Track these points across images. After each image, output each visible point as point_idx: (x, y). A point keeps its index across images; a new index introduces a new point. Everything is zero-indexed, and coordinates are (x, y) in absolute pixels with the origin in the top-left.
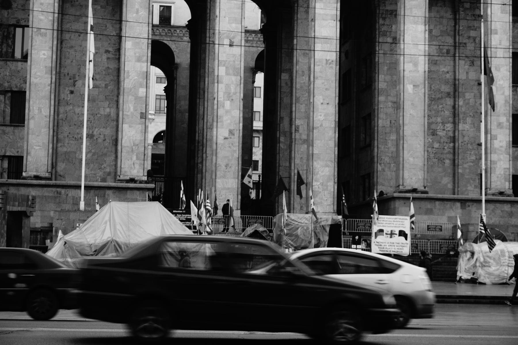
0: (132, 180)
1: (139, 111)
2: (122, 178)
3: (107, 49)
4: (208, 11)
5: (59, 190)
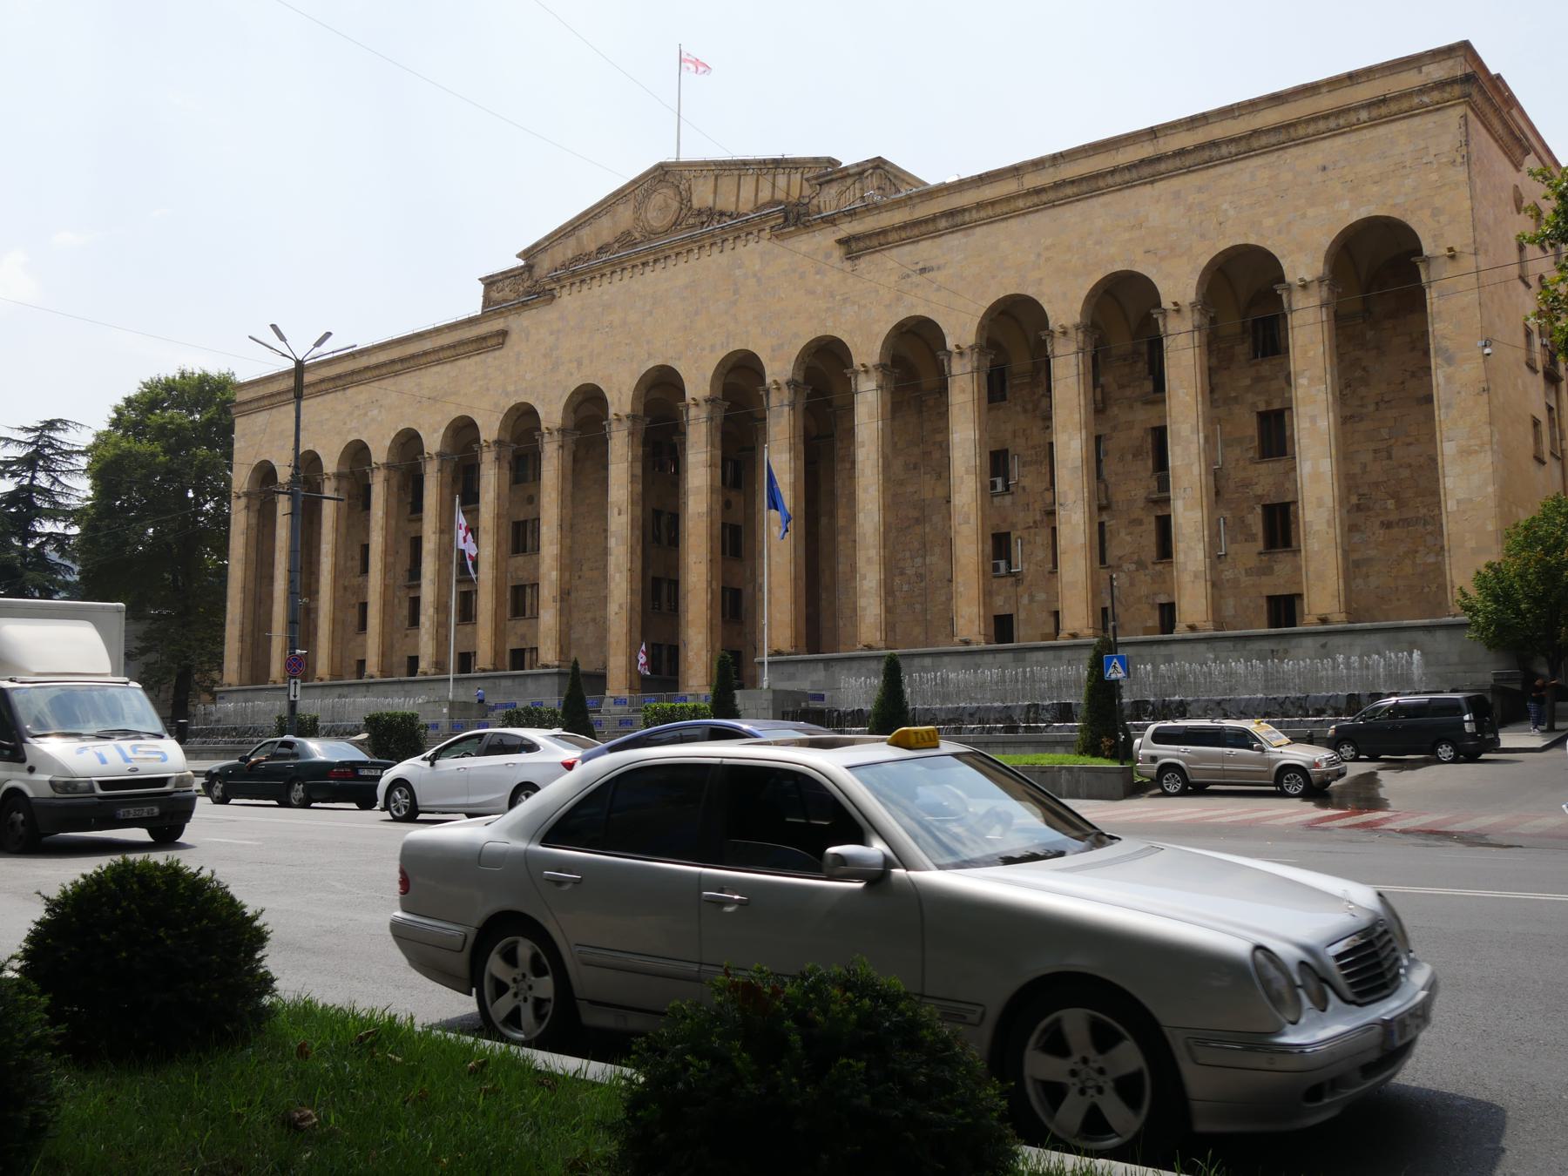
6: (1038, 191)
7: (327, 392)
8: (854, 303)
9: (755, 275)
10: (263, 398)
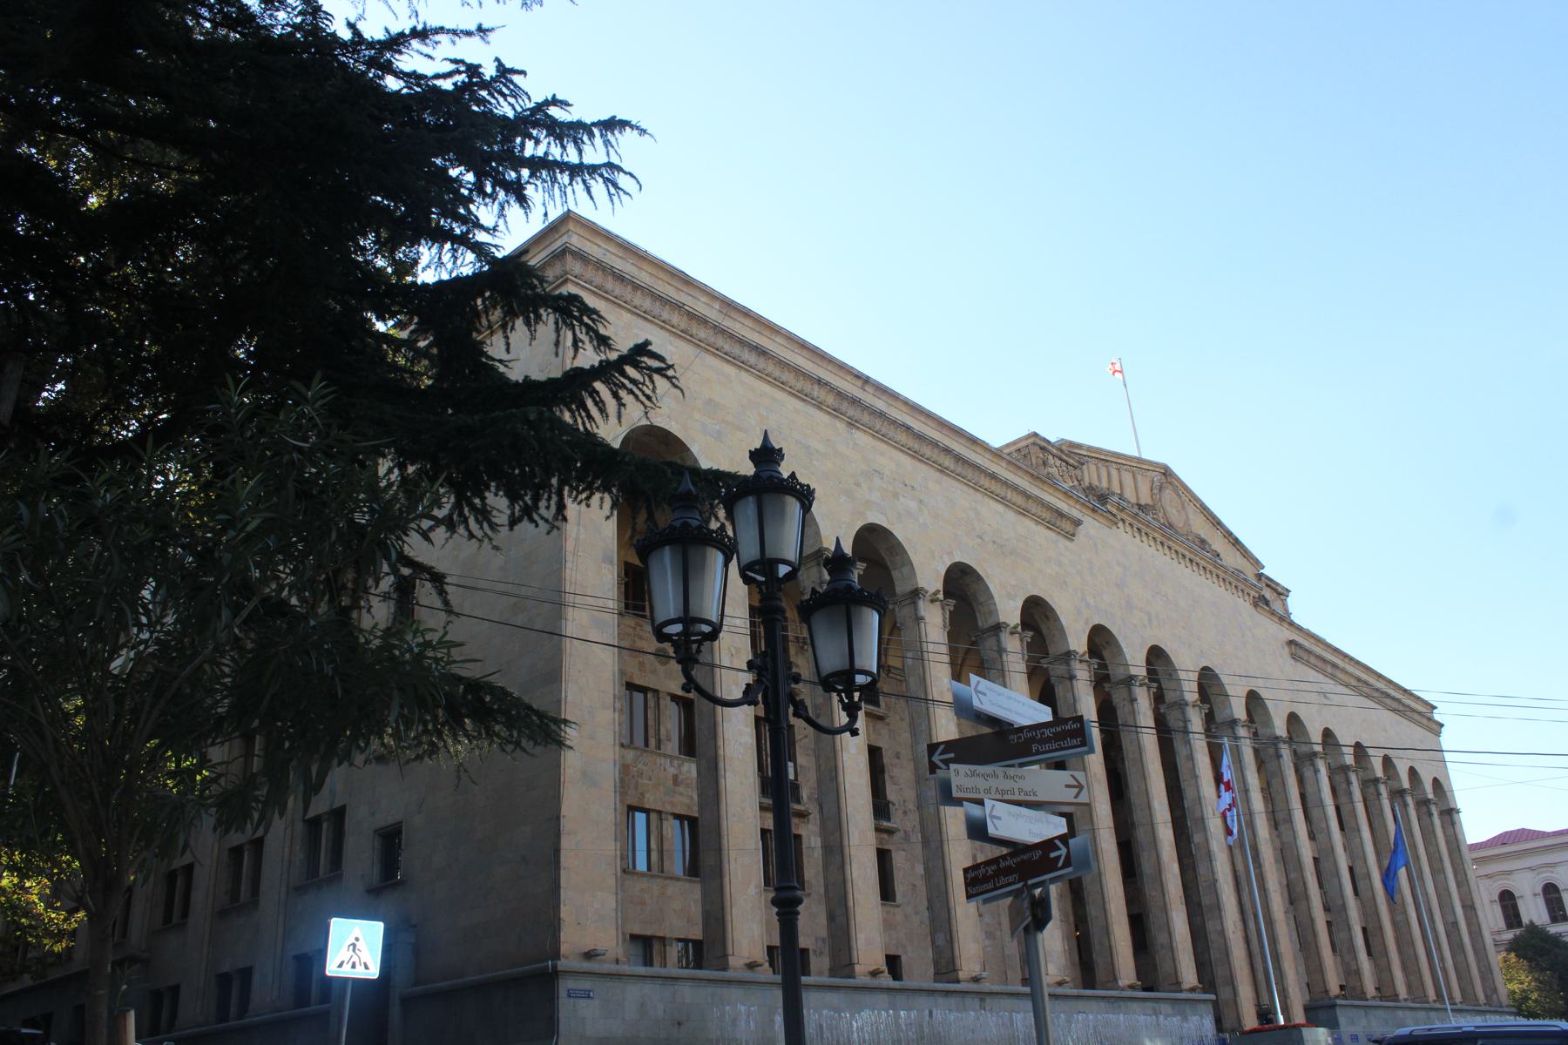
7: (819, 405)
10: (678, 307)
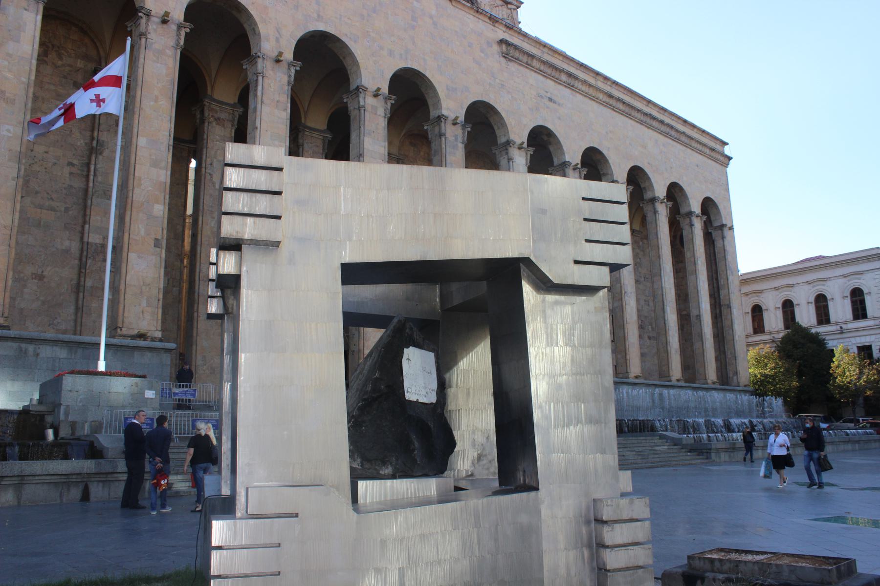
0: (142, 336)
1: (153, 237)
2: (125, 331)
3: (70, 160)
4: (205, 136)
5: (23, 345)
6: (610, 96)
8: (509, 92)
9: (431, 17)
